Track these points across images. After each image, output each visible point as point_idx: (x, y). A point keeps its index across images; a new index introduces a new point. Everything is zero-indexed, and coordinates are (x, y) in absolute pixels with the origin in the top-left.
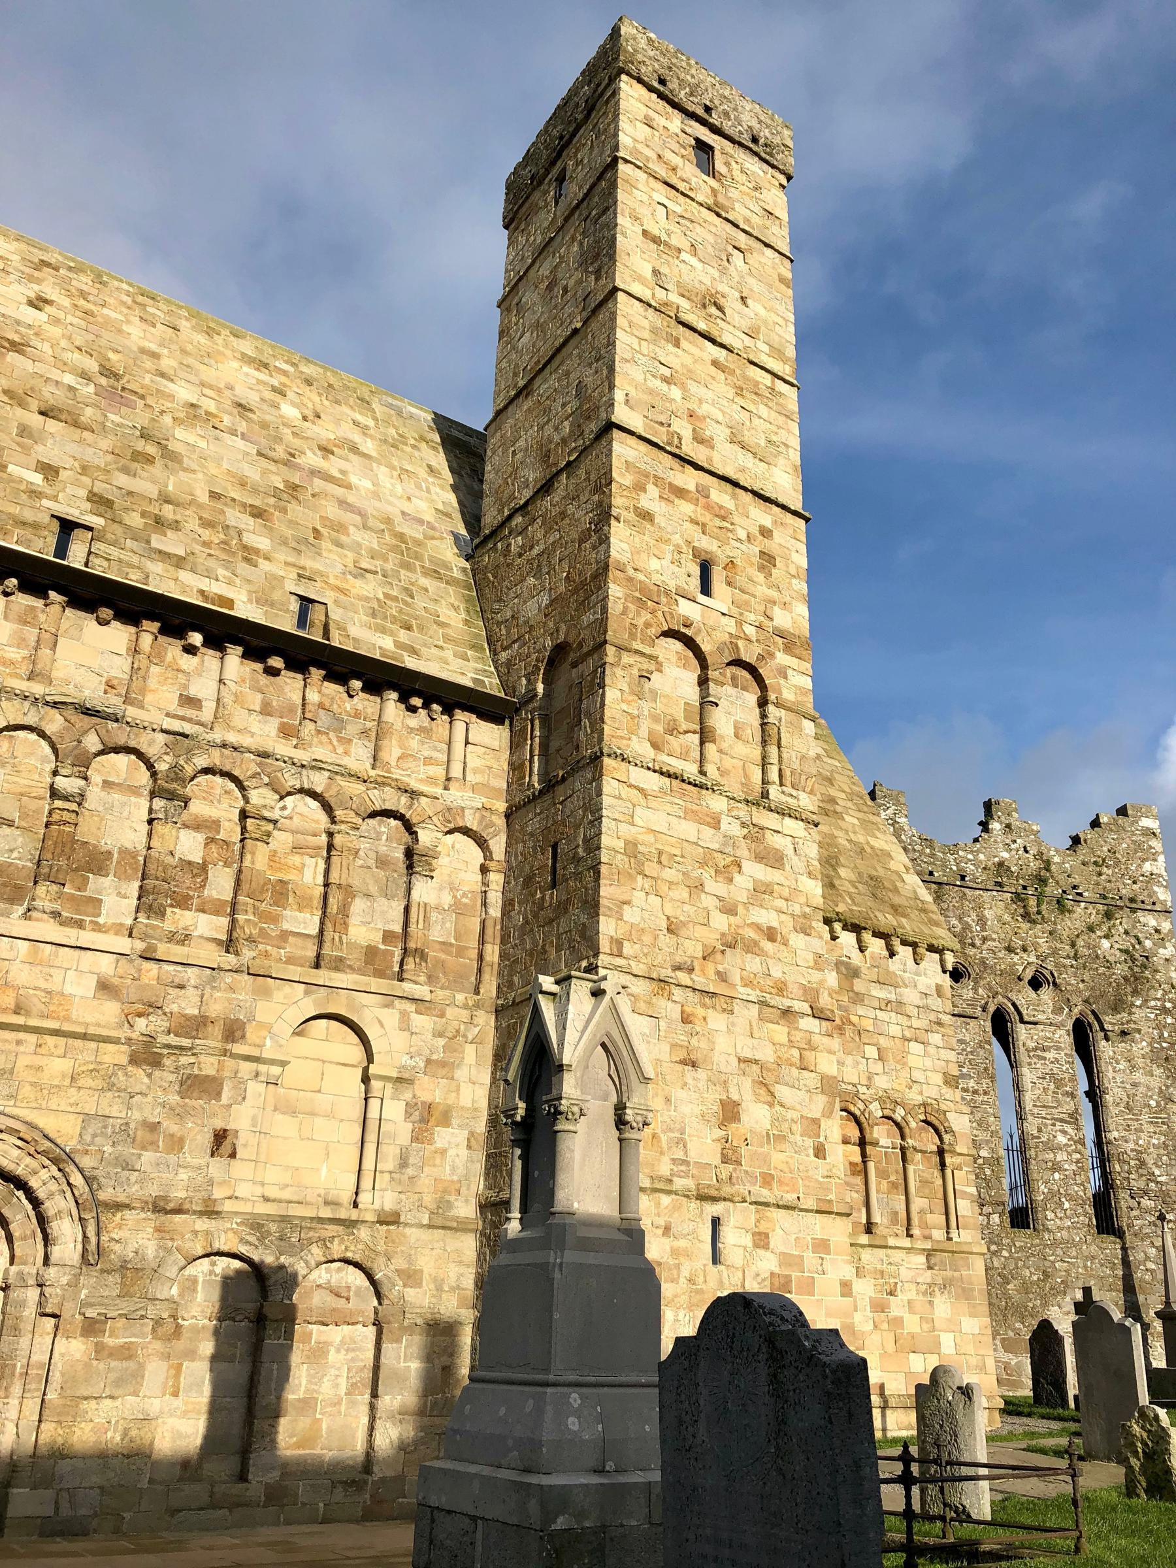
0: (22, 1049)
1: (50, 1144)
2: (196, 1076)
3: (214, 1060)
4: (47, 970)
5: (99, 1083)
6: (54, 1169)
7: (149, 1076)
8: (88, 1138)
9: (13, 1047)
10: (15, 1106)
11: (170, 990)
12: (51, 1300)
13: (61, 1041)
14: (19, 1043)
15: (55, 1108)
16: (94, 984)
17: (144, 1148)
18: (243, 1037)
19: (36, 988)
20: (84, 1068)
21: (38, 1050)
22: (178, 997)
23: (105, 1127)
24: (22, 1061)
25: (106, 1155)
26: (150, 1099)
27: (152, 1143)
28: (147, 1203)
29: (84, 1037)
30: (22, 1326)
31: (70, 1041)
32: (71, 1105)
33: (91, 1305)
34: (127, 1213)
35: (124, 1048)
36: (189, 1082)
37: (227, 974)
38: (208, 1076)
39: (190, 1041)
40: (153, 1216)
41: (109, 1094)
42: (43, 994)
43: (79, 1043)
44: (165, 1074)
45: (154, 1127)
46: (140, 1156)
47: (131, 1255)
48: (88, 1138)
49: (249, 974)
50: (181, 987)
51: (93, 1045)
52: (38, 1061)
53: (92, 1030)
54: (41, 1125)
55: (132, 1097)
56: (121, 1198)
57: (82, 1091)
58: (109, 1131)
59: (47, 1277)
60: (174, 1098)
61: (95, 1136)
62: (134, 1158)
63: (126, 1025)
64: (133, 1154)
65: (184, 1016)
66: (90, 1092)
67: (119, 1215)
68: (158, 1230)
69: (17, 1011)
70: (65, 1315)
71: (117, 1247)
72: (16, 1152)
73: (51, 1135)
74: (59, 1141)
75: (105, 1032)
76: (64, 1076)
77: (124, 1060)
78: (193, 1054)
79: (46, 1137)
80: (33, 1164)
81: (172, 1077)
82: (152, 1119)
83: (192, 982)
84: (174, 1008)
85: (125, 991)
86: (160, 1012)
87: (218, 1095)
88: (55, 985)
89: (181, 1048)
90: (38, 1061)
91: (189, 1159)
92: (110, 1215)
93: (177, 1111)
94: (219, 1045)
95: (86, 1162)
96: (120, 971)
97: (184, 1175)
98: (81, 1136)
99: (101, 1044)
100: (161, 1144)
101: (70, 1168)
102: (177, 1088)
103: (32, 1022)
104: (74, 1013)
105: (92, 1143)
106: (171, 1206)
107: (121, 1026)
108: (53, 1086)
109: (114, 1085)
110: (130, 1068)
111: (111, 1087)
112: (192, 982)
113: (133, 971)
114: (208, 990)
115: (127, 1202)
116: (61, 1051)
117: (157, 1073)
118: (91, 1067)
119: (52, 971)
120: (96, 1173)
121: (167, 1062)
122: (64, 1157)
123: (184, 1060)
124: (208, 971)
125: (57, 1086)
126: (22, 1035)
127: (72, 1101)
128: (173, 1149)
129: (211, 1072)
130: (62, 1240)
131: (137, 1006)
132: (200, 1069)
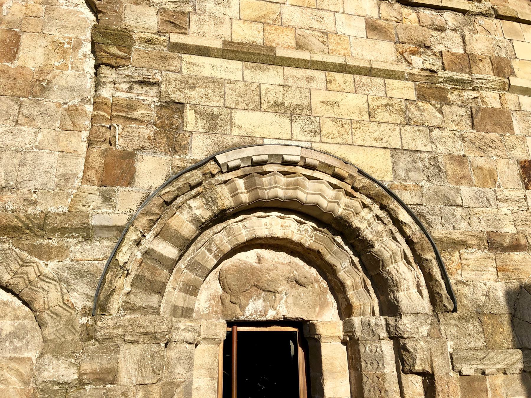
0: (313, 85)
1: (368, 181)
2: (484, 109)
3: (494, 95)
4: (316, 12)
5: (396, 118)
6: (376, 208)
7: (440, 111)
8: (402, 173)
9: (304, 84)
10: (321, 142)
11: (433, 33)
12: (418, 356)
13: (349, 77)
14: (309, 79)
15: (360, 143)
16: (364, 25)
17: (457, 182)
18: (513, 73)
19: (311, 29)
20: (378, 103)
21: (329, 86)
22: (442, 38)
23: (415, 161)
24: (318, 97)
25: (425, 191)
26: (447, 133)
27: (464, 177)
28: (481, 239)
29: (370, 72)
30: (387, 386)
31: (357, 77)
32: (376, 140)
33: (465, 360)
34: (466, 253)
35: (410, 84)
36: (480, 115)
37: (478, 18)
38: (494, 110)
39: (468, 76)
40: (492, 255)
41: (409, 128)
42: (320, 35)
43: (365, 79)
44: (455, 109)
45: (461, 160)
46: (458, 191)
47: (483, 298)
48: (402, 173)
49: (499, 17)
50: (441, 29)
51: (379, 81)
52: (332, 96)
53: (375, 65)
54: (353, 161)
55: (431, 131)
56: (456, 235)
57: (382, 125)
58: (420, 165)
59: (403, 327)
60: (471, 134)
61: (408, 171)
62: (453, 192)
63: (404, 63)
64: (451, 189)
65: (453, 54)
66: (390, 126)
67: (457, 254)
68: (498, 269)
69: (299, 47)
70: (439, 373)
71: (466, 290)
72: (331, 193)
73: (365, 170)
74: (374, 176)
75: (389, 67)
76: (361, 112)
77: (413, 96)
78: (474, 90)
79: (360, 172)
80: (355, 204)
81: (462, 111)
82: (456, 153)
83: (450, 24)
84: (441, 48)
85: (393, 32)
86: (430, 53)
87: (510, 127)
88: (328, 23)
89: (462, 82)
90: (332, 96)
91: (506, 192)
92: (447, 255)
93: (477, 144)
94: (497, 79)
95: (407, 198)
96: (384, 14)
97: (504, 209)
98: (394, 171)
99: (387, 81)
100: (473, 178)
101: (394, 205)
102: (469, 122)
103: (318, 57)
104: (354, 52)
105: (407, 179)
106: (507, 242)
107: (399, 61)
108: (352, 122)
109: (410, 119)
110: (420, 104)
111: (408, 121)
112: (450, 24)
113: (395, 14)
114: (466, 32)
115: (462, 238)
116: (352, 88)
117: (446, 108)
118: (384, 102)
119: (322, 13)
120: (421, 209)
121: (452, 97)
122: (385, 193)
123: (468, 95)
124: (460, 15)
125: (357, 121)
126: (309, 72)
127: (376, 135)
128: (487, 183)
129: (497, 105)
130: (404, 286)
131: (408, 46)
132: (485, 103)
